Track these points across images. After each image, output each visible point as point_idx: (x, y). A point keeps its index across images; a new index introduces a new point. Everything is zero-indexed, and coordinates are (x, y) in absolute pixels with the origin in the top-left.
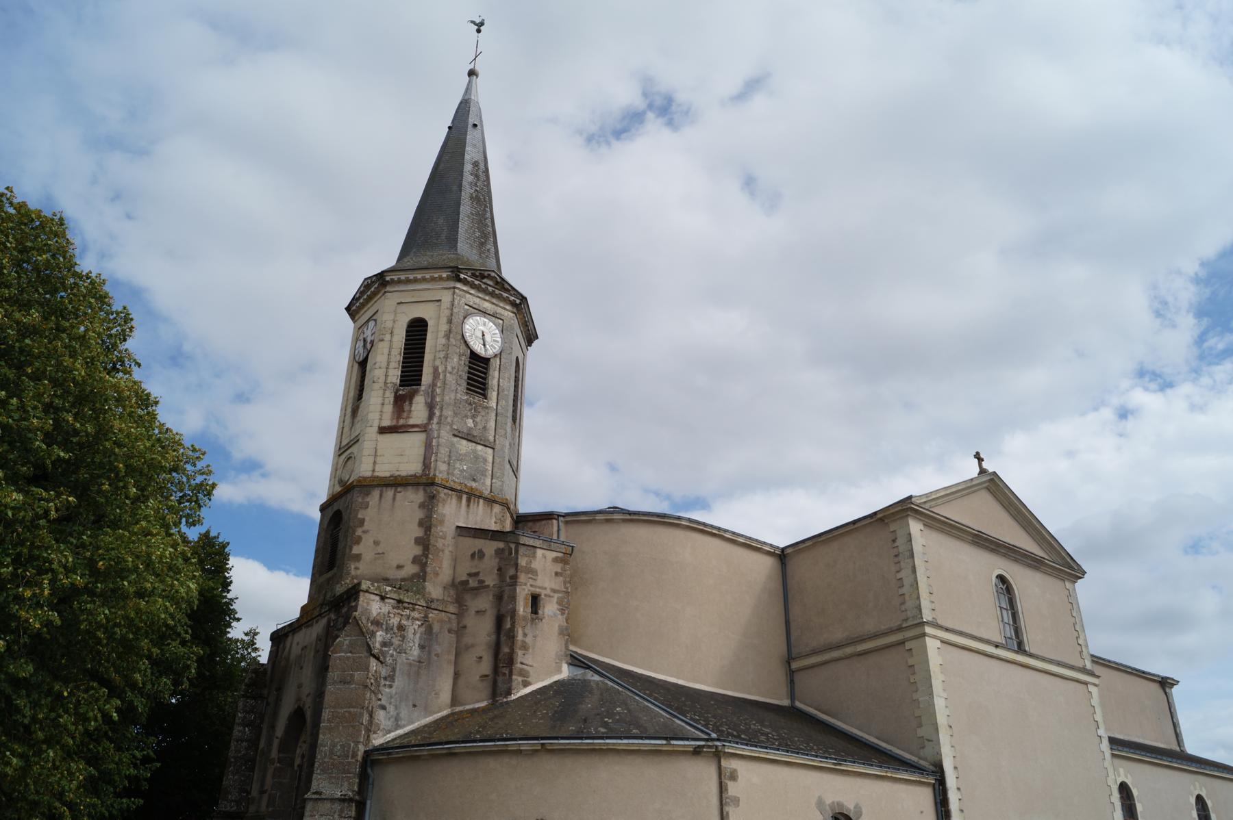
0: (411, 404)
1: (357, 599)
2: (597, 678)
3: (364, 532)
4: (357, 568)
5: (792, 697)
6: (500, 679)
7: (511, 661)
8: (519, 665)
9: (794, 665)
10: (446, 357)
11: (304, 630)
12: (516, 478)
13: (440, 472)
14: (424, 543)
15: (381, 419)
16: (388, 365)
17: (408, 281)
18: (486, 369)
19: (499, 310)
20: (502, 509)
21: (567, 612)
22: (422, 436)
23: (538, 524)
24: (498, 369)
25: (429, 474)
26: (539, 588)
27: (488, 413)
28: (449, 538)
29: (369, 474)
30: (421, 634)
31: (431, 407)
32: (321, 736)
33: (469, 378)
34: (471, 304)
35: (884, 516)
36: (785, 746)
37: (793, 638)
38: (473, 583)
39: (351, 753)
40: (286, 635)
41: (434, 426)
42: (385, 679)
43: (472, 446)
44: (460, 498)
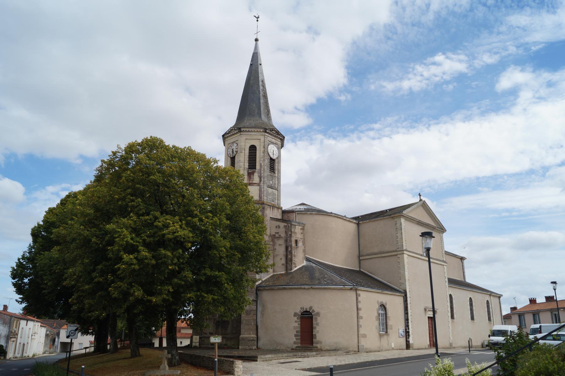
0: (253, 176)
5: (360, 268)
7: (291, 260)
8: (293, 261)
9: (361, 258)
10: (264, 160)
13: (265, 200)
16: (244, 161)
17: (249, 131)
19: (277, 142)
22: (258, 187)
23: (289, 214)
25: (261, 201)
31: (260, 177)
33: (270, 167)
34: (269, 140)
35: (394, 217)
36: (369, 287)
37: (360, 250)
38: (277, 235)
41: (262, 184)
44: (270, 208)
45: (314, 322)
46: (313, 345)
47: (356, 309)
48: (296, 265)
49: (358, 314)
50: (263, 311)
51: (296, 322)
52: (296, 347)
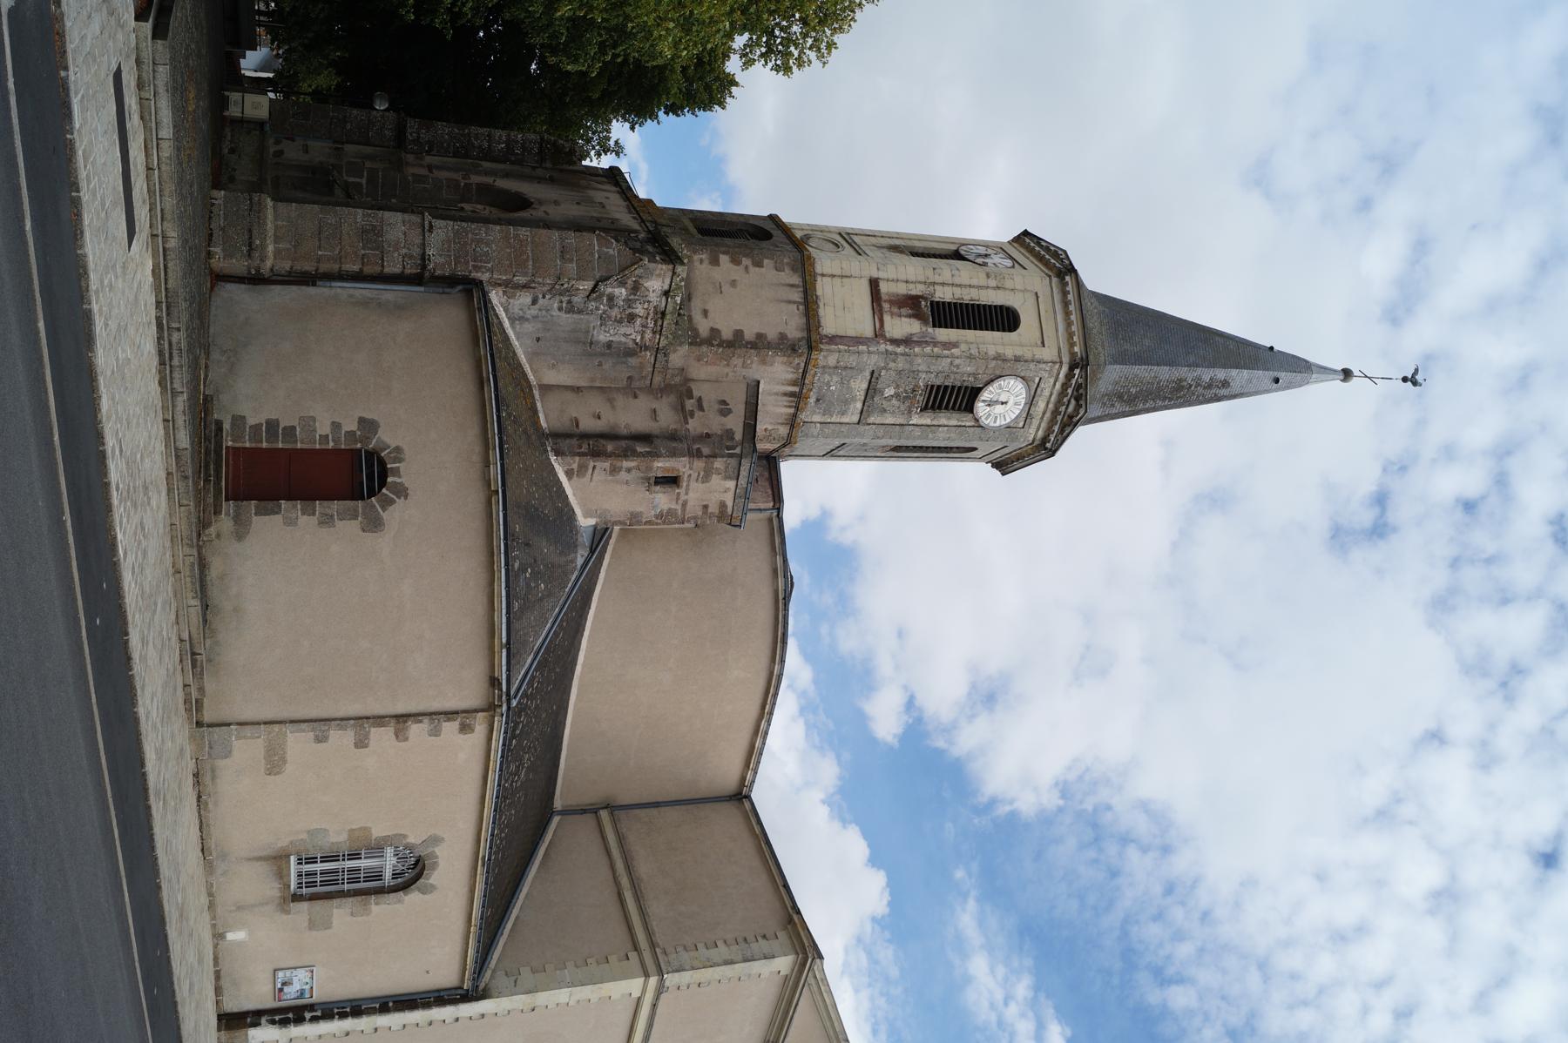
0: (910, 316)
1: (664, 261)
2: (580, 561)
3: (747, 268)
4: (701, 261)
5: (565, 812)
6: (574, 442)
7: (597, 454)
9: (604, 814)
10: (971, 357)
11: (624, 204)
12: (824, 455)
13: (825, 357)
14: (736, 342)
15: (888, 280)
16: (957, 285)
17: (1066, 304)
18: (959, 409)
19: (1035, 422)
20: (783, 438)
21: (659, 521)
22: (868, 331)
23: (767, 484)
24: (960, 423)
25: (821, 343)
26: (688, 486)
27: (903, 414)
28: (745, 372)
29: (819, 269)
30: (625, 343)
31: (907, 341)
32: (498, 227)
33: (946, 387)
34: (1042, 385)
35: (795, 924)
36: (503, 796)
37: (637, 811)
38: (690, 404)
39: (480, 264)
40: (617, 184)
41: (883, 346)
42: (569, 302)
43: (861, 395)
44: (794, 383)
45: (335, 506)
46: (227, 499)
47: (401, 709)
48: (575, 478)
49: (379, 720)
50: (379, 305)
51: (336, 426)
52: (219, 424)
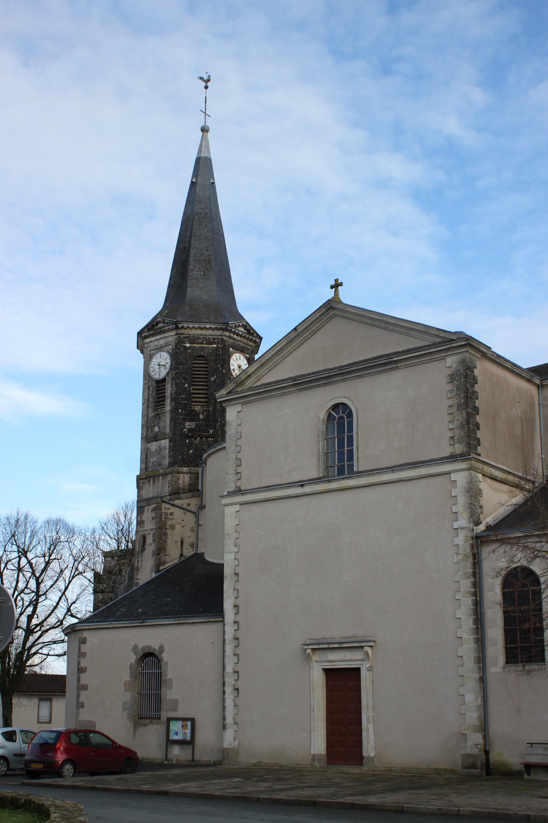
8: (135, 581)
